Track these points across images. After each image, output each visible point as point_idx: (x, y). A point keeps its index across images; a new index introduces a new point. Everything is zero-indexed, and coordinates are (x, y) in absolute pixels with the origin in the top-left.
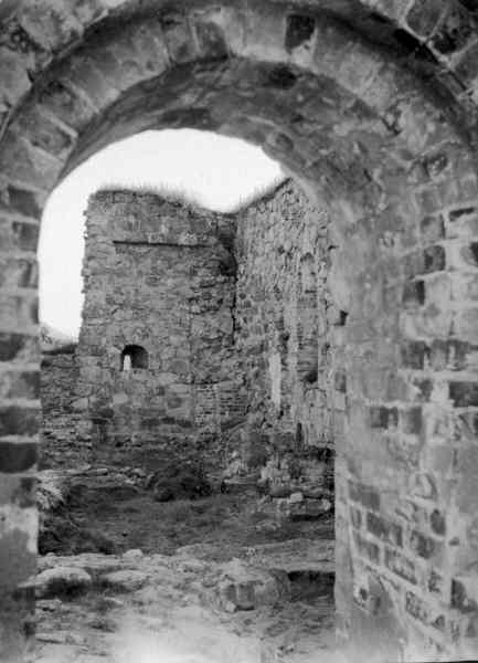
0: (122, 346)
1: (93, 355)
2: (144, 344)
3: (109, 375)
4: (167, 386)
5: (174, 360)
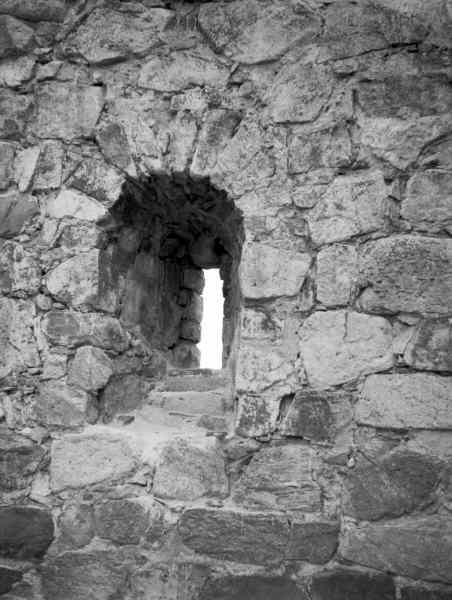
0: (112, 184)
3: (41, 326)
4: (350, 389)
5: (385, 244)
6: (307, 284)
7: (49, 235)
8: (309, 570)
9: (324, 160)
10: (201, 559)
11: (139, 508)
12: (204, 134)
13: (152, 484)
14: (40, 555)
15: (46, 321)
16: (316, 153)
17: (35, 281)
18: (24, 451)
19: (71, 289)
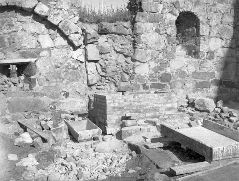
1: (150, 22)
2: (195, 11)
6: (210, 33)
7: (166, 22)
8: (211, 80)
9: (212, 11)
10: (195, 80)
11: (185, 72)
12: (194, 4)
13: (187, 68)
14: (169, 81)
15: (167, 39)
16: (211, 9)
17: (165, 31)
18: (166, 63)
19: (171, 33)
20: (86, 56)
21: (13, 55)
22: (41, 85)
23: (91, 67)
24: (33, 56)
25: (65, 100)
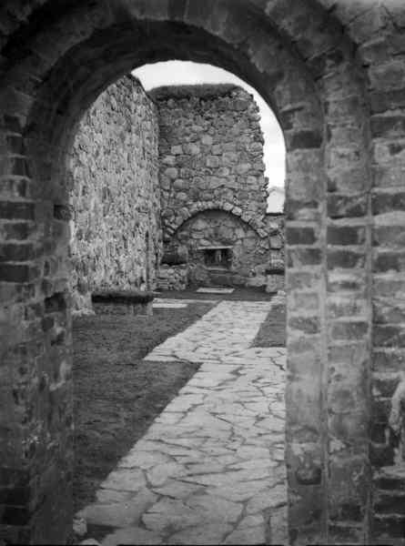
20: (270, 245)
21: (215, 243)
22: (235, 265)
23: (273, 254)
24: (230, 244)
25: (253, 279)
